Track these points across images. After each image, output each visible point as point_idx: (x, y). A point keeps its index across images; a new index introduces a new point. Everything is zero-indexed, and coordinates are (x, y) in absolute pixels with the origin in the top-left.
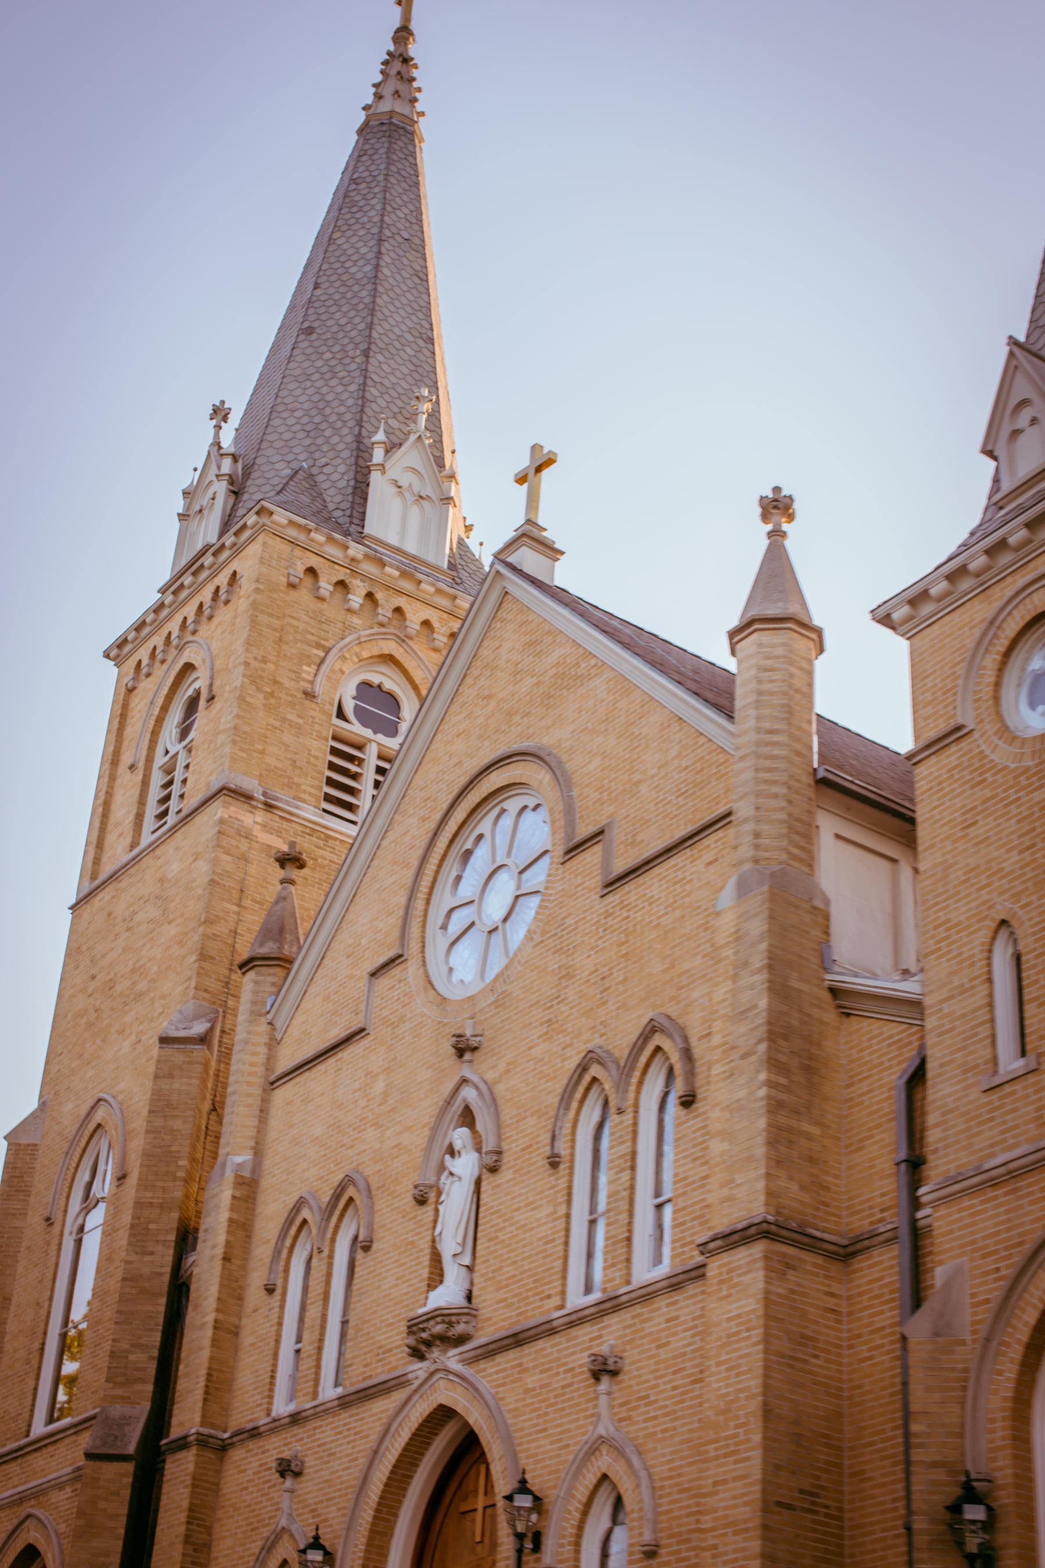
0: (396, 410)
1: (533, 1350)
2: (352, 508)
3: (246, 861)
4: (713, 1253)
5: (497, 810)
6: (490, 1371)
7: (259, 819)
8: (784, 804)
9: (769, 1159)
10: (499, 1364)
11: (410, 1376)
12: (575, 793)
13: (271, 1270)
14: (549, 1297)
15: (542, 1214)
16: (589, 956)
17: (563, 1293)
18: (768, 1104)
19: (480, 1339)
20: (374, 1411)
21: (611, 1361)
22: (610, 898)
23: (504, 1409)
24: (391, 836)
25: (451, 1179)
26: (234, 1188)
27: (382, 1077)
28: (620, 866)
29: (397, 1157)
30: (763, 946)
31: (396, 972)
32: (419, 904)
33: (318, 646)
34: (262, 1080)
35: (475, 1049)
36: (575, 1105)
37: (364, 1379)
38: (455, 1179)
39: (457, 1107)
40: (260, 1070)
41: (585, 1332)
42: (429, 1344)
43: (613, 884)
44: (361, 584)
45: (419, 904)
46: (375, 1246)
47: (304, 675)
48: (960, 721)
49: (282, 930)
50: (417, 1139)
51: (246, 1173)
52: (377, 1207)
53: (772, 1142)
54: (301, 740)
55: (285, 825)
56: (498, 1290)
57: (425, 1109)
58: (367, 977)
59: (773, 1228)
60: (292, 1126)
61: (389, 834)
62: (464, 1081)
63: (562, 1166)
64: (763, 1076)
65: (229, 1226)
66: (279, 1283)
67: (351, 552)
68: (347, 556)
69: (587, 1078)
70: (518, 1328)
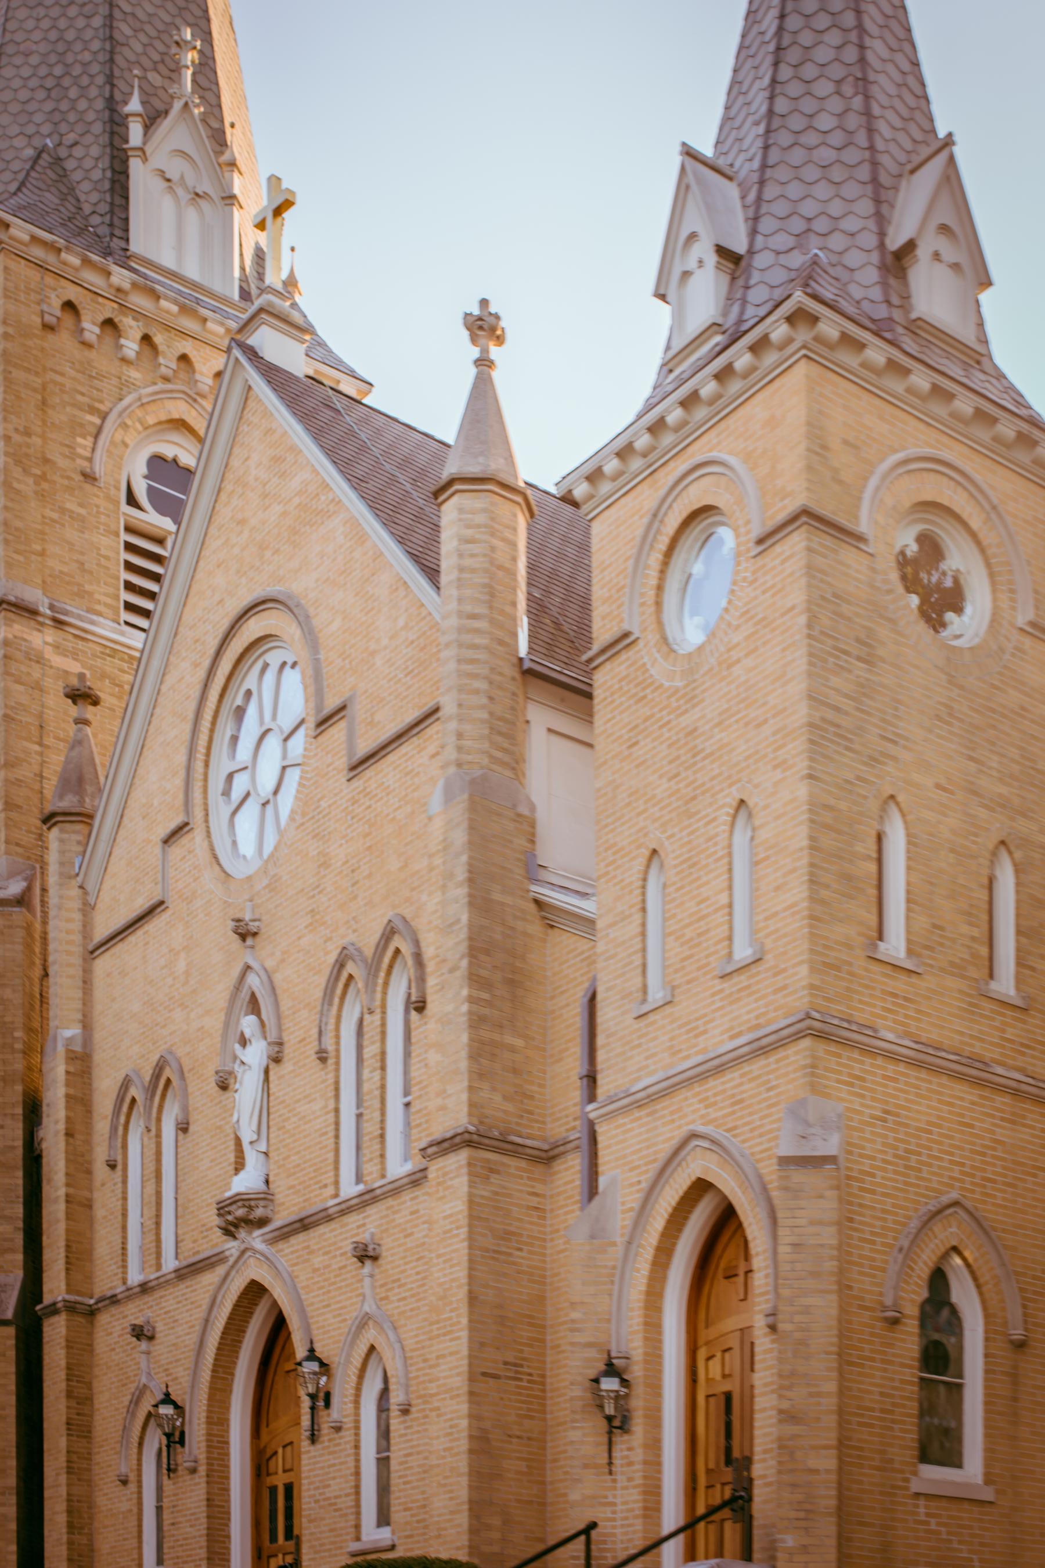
0: (156, 57)
2: (112, 212)
3: (41, 690)
4: (432, 1158)
7: (49, 639)
8: (485, 701)
9: (470, 1072)
11: (227, 1253)
12: (322, 657)
13: (110, 1147)
14: (325, 1186)
17: (337, 1183)
18: (470, 1020)
19: (277, 1223)
21: (371, 1247)
23: (299, 1286)
25: (243, 1068)
26: (67, 1063)
27: (183, 955)
30: (464, 858)
31: (184, 840)
32: (199, 766)
33: (92, 410)
35: (255, 934)
36: (336, 1001)
39: (245, 995)
40: (77, 938)
41: (353, 1220)
42: (236, 1226)
44: (133, 323)
45: (199, 766)
47: (80, 451)
48: (626, 627)
49: (80, 780)
50: (215, 1023)
51: (78, 1048)
53: (474, 1056)
54: (86, 536)
56: (289, 1176)
57: (219, 993)
58: (160, 844)
59: (475, 1137)
61: (167, 677)
64: (465, 992)
65: (67, 1102)
66: (119, 1158)
67: (115, 280)
70: (303, 1214)
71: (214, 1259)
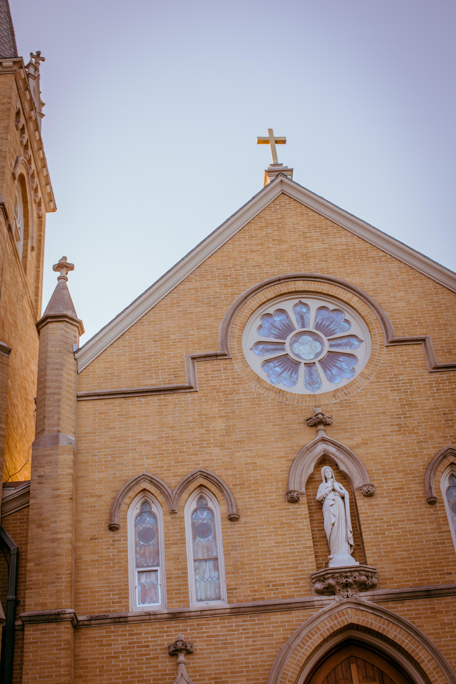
1: (443, 601)
6: (399, 609)
14: (450, 574)
15: (429, 527)
16: (429, 400)
20: (272, 620)
22: (438, 375)
29: (253, 470)
31: (221, 364)
37: (254, 600)
43: (437, 369)
46: (242, 519)
62: (323, 440)
70: (431, 588)
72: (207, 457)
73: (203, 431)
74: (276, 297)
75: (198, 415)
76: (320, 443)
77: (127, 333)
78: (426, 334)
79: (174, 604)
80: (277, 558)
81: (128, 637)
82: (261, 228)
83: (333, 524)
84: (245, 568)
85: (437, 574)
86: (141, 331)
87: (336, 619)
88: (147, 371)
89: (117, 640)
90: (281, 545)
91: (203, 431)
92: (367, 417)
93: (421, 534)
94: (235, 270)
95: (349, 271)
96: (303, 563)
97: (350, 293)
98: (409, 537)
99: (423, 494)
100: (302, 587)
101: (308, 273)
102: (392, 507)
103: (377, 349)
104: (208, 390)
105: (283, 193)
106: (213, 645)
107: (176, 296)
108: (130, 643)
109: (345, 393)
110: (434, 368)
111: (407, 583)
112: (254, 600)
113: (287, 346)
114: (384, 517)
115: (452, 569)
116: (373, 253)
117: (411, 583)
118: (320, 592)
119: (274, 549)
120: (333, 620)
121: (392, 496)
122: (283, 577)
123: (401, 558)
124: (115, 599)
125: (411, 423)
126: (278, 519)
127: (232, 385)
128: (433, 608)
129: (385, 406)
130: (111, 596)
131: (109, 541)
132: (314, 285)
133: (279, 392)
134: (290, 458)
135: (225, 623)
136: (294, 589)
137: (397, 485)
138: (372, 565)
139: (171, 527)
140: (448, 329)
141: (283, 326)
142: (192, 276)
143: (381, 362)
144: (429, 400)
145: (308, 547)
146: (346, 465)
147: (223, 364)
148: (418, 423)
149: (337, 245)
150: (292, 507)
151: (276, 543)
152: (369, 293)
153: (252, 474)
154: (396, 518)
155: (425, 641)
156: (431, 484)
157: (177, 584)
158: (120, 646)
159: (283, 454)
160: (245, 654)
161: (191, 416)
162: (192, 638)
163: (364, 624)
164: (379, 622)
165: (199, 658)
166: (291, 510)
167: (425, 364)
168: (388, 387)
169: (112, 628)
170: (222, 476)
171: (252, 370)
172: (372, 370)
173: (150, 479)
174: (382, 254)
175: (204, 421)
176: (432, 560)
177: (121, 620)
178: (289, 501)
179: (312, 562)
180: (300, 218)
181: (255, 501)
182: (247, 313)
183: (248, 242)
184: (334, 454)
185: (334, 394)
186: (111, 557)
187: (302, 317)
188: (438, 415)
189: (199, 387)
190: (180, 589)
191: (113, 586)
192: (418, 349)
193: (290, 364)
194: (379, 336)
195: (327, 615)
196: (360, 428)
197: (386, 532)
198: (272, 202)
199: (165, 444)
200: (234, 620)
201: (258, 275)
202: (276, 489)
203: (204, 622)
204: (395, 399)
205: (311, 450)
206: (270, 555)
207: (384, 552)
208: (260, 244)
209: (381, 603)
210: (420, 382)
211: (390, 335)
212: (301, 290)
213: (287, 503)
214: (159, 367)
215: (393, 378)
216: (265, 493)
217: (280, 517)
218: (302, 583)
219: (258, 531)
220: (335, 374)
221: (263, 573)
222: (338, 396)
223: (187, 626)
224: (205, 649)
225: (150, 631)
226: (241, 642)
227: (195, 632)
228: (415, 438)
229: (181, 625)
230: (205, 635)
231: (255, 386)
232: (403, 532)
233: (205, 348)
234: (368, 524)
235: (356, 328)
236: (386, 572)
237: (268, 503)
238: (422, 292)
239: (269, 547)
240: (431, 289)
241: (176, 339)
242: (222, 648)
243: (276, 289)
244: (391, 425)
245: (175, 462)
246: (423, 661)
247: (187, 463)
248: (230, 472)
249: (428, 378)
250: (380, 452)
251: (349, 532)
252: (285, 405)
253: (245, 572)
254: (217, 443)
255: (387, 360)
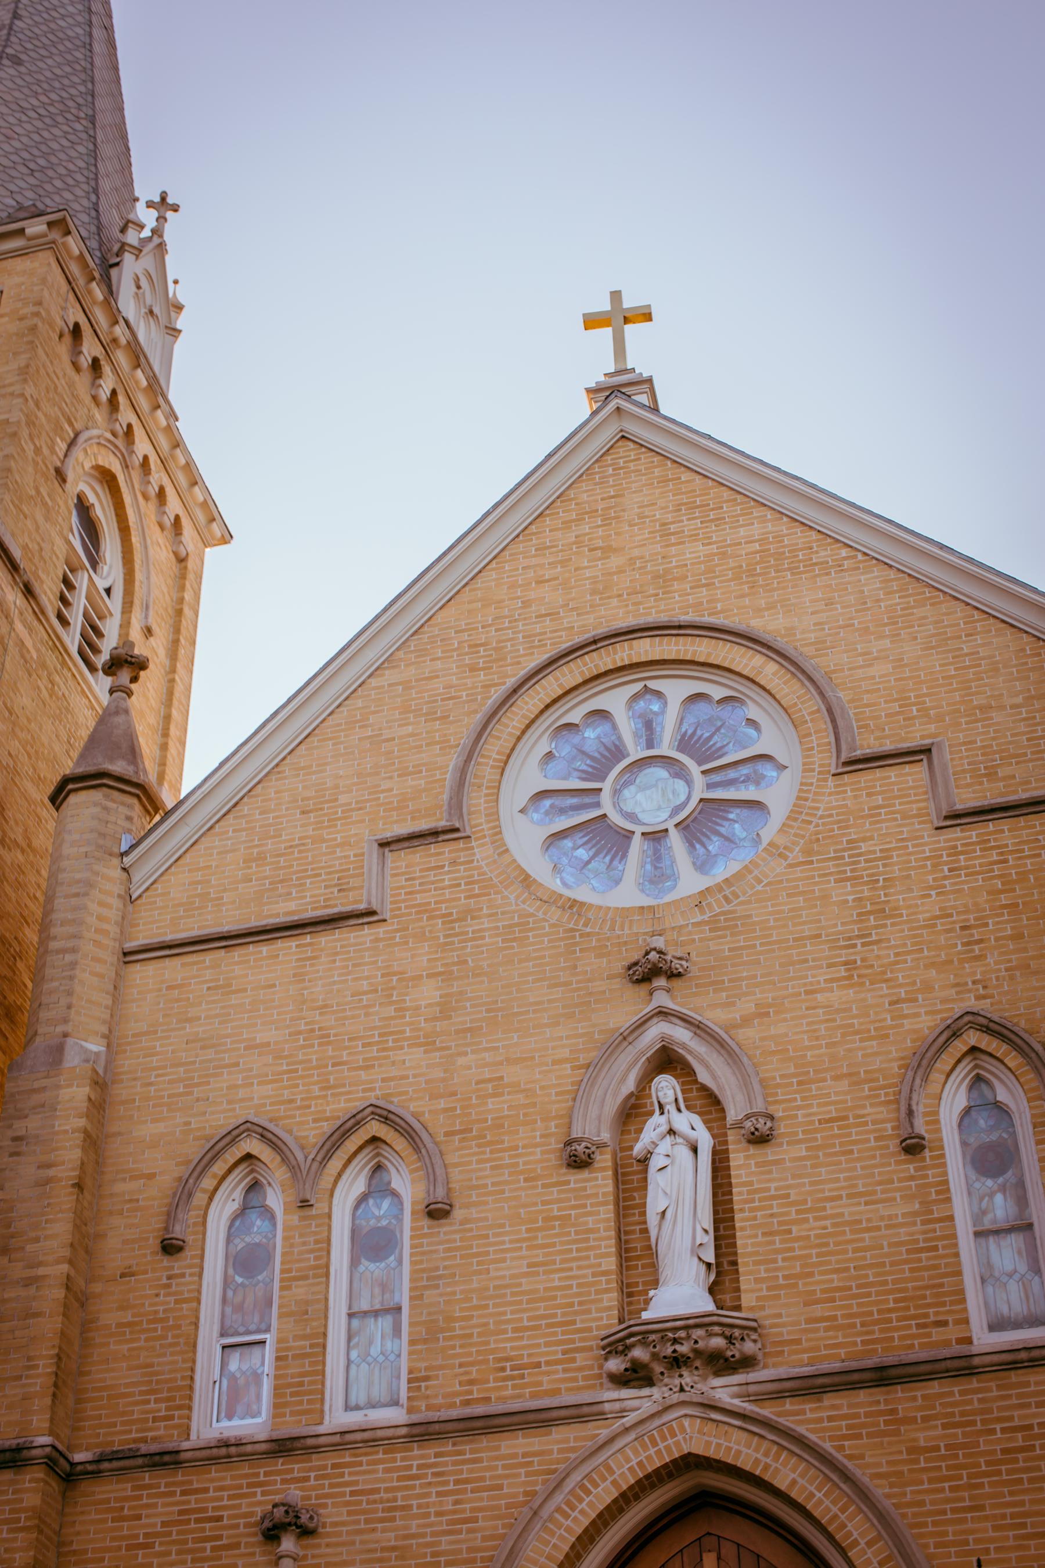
1: (919, 1394)
5: (638, 687)
6: (809, 1415)
10: (833, 1407)
14: (945, 1323)
16: (930, 896)
20: (504, 1451)
24: (390, 676)
28: (967, 799)
29: (494, 1095)
34: (117, 945)
37: (467, 1403)
38: (679, 1140)
43: (956, 818)
46: (458, 1214)
52: (450, 1159)
55: (36, 623)
56: (806, 1304)
60: (189, 1020)
62: (662, 1013)
63: (927, 1153)
68: (111, 333)
69: (960, 1046)
71: (586, 1410)
72: (394, 1072)
73: (390, 1011)
74: (586, 682)
75: (383, 976)
76: (655, 1020)
77: (245, 799)
78: (935, 736)
79: (288, 1418)
80: (529, 1302)
81: (178, 1498)
82: (567, 524)
83: (664, 1212)
84: (454, 1329)
85: (910, 1327)
86: (276, 792)
87: (655, 1444)
88: (282, 881)
89: (155, 1506)
90: (541, 1269)
91: (390, 1011)
92: (773, 951)
93: (878, 1228)
94: (497, 630)
95: (763, 603)
96: (589, 1311)
97: (758, 656)
98: (849, 1237)
99: (893, 1129)
100: (580, 1369)
101: (663, 618)
102: (813, 1166)
103: (812, 784)
104: (410, 914)
105: (623, 437)
106: (364, 1512)
107: (360, 703)
108: (181, 1513)
109: (726, 898)
110: (946, 818)
111: (832, 1349)
112: (467, 1403)
113: (606, 797)
114: (792, 1192)
115: (949, 1312)
116: (823, 553)
117: (842, 1351)
118: (621, 1380)
119: (524, 1280)
120: (645, 1448)
121: (816, 1139)
122: (538, 1345)
123: (823, 1291)
124: (160, 1411)
125: (878, 957)
126: (540, 1207)
127: (466, 898)
128: (893, 1411)
129: (819, 921)
130: (152, 1405)
131: (160, 1279)
132: (676, 644)
133: (571, 907)
134: (582, 1062)
135: (394, 1460)
136: (561, 1375)
137: (830, 1112)
138: (751, 1309)
139: (297, 1240)
140: (991, 718)
141: (602, 749)
142: (401, 654)
143: (820, 813)
144: (930, 896)
145: (604, 1273)
146: (712, 1070)
147: (450, 852)
148: (897, 954)
149: (740, 544)
150: (576, 1178)
151: (529, 1266)
152: (805, 650)
153: (491, 1104)
154: (823, 1191)
155: (863, 1494)
156: (914, 1103)
157: (302, 1375)
158: (158, 1520)
159: (566, 1053)
160: (434, 1534)
161: (367, 978)
162: (317, 1497)
163: (720, 1456)
164: (756, 1450)
165: (328, 1545)
166: (572, 1185)
167: (927, 808)
168: (831, 874)
169: (147, 1478)
170: (423, 1113)
171: (515, 861)
172: (796, 835)
173: (260, 1130)
174: (844, 553)
175: (393, 988)
176: (900, 1290)
177: (166, 1458)
178: (569, 1165)
179: (610, 1308)
180: (657, 491)
181: (492, 1168)
182: (514, 727)
183: (534, 561)
184: (684, 1046)
185: (700, 900)
186: (161, 1315)
187: (649, 725)
188: (948, 931)
189: (392, 910)
190: (301, 1384)
191: (158, 1382)
192: (914, 774)
193: (608, 838)
194: (820, 752)
195: (632, 1436)
196: (755, 977)
197: (794, 1228)
198: (597, 461)
199: (304, 1047)
200: (416, 1452)
201: (549, 635)
202: (542, 1136)
203: (347, 1459)
204: (847, 901)
205: (630, 1039)
206: (513, 1294)
207: (785, 1277)
208: (561, 562)
209: (767, 1403)
210: (910, 854)
211: (844, 747)
212: (644, 659)
213: (564, 1170)
214: (306, 870)
215: (844, 850)
216: (516, 1148)
217: (544, 1203)
218: (581, 1359)
219: (492, 1240)
220: (714, 852)
221: (493, 1338)
222: (709, 905)
223: (310, 1470)
224: (343, 1524)
225: (228, 1482)
226: (428, 1505)
227: (327, 1482)
228: (886, 991)
229: (297, 1468)
230: (348, 1489)
231: (517, 897)
232: (834, 1225)
233: (413, 819)
234: (751, 1210)
235: (772, 738)
236: (783, 1325)
237: (521, 1172)
238: (933, 635)
239: (512, 1277)
240: (958, 624)
241: (350, 804)
242: (382, 1520)
243: (585, 665)
244: (829, 966)
245: (322, 1089)
246: (856, 1543)
247: (347, 1089)
248: (442, 1104)
249: (933, 842)
250: (797, 1033)
251: (699, 1232)
252: (581, 936)
253: (451, 1338)
254: (419, 1037)
255: (833, 808)
